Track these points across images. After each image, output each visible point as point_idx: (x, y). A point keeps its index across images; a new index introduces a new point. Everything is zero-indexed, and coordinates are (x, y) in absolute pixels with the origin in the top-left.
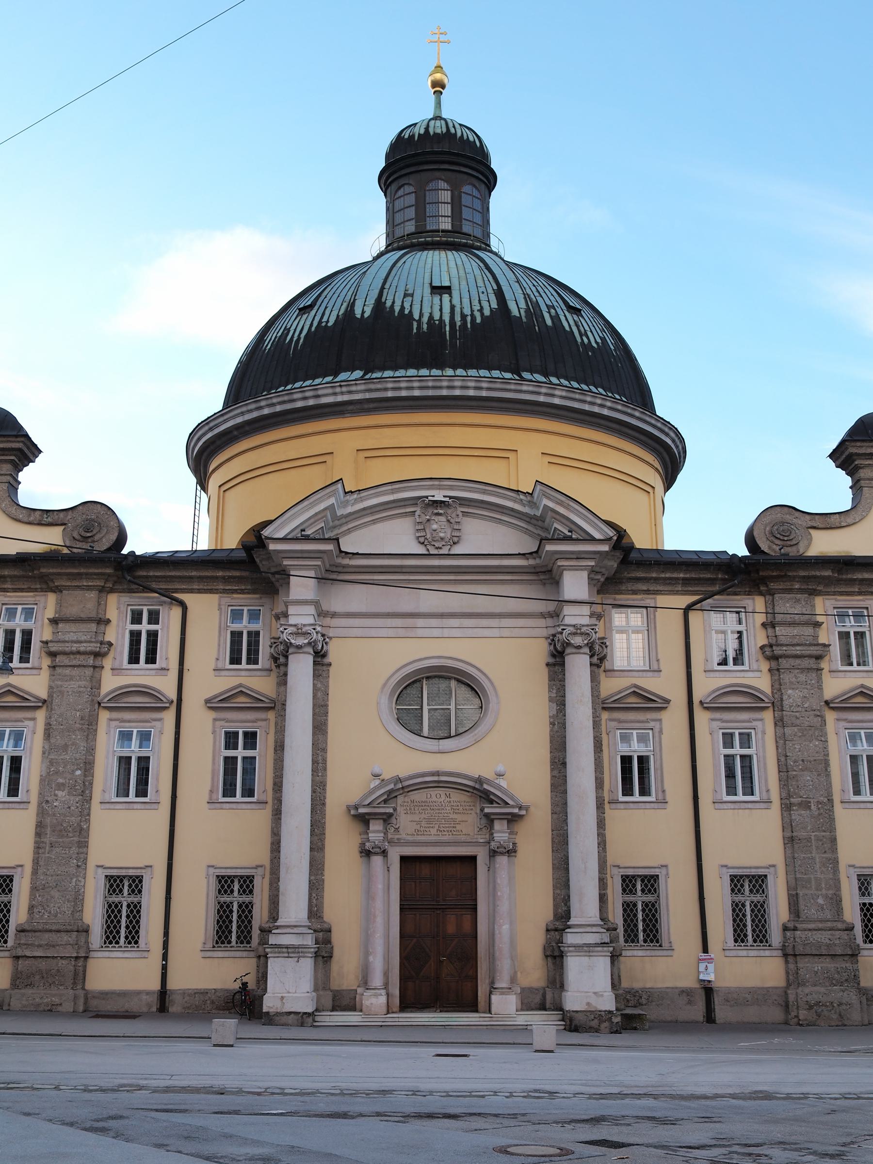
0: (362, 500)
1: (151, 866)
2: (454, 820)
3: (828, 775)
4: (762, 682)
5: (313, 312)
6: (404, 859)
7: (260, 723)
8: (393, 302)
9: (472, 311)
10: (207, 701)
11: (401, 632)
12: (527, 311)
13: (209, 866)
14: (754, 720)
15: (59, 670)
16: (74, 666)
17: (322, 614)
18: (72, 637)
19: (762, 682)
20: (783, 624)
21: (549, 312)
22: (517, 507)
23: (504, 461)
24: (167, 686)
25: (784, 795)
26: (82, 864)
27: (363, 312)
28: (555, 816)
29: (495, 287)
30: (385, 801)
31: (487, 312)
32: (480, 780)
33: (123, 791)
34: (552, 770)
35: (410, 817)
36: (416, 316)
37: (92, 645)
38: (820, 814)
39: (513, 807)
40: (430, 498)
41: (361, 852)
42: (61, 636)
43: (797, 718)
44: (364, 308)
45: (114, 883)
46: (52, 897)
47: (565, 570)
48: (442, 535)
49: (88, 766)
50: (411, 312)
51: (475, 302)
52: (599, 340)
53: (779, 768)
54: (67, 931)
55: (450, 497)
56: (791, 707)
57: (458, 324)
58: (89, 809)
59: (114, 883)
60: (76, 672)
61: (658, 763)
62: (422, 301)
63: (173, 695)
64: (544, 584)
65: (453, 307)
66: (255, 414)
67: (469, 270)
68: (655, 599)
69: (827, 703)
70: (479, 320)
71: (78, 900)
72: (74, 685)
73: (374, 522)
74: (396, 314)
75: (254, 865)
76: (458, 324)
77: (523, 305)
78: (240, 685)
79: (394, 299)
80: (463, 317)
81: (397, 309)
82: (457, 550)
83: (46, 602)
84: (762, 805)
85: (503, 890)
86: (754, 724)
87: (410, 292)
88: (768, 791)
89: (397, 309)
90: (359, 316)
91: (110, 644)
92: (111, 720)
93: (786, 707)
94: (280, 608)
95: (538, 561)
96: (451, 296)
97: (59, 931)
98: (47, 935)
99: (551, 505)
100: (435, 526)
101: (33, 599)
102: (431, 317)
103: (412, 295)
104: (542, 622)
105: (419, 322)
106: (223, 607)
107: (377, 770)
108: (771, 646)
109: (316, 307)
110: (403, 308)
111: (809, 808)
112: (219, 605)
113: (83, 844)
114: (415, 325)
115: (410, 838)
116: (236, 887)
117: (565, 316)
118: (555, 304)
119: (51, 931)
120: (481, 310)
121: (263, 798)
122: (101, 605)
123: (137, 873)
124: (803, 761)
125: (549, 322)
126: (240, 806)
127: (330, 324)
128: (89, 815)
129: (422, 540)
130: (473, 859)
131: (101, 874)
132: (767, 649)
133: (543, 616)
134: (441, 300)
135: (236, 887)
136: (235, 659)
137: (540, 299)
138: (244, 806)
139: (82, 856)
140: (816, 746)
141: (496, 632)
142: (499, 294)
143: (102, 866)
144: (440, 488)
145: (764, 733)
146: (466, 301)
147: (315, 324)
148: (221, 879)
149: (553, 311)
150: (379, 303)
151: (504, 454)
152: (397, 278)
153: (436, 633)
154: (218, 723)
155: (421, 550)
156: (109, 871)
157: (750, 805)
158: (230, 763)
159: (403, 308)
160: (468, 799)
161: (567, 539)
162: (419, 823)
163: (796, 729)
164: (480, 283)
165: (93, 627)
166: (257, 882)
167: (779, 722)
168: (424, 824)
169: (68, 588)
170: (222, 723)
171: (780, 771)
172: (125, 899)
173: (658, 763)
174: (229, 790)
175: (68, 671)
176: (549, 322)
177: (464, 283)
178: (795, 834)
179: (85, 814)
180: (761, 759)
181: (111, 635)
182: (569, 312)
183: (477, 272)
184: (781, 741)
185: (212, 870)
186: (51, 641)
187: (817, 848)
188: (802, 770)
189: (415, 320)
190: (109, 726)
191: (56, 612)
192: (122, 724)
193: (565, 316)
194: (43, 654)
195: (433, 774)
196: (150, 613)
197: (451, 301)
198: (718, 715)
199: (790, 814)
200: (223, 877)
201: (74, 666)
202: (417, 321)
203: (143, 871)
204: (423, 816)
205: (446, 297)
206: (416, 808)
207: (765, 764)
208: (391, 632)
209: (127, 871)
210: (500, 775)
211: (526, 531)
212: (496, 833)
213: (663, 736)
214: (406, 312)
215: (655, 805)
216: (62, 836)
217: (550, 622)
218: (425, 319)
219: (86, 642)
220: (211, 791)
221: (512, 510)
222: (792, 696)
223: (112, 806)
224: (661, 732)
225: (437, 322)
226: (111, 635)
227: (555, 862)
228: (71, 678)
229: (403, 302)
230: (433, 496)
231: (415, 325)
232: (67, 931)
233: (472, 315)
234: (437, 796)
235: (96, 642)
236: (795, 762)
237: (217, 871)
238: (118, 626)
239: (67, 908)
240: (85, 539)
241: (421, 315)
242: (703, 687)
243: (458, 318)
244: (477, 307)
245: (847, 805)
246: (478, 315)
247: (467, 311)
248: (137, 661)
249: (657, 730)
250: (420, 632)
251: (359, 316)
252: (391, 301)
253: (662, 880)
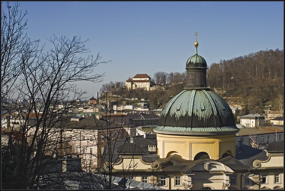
5: (180, 111)
27: (190, 115)
31: (211, 115)
36: (199, 117)
44: (190, 114)
65: (205, 114)
79: (195, 112)
81: (196, 114)
89: (196, 114)
102: (202, 116)
109: (180, 110)
110: (197, 114)
120: (210, 115)
127: (184, 116)
142: (212, 109)
147: (181, 115)
159: (197, 114)
164: (209, 108)
196: (164, 177)
214: (197, 115)
218: (201, 117)
243: (206, 117)
246: (209, 115)
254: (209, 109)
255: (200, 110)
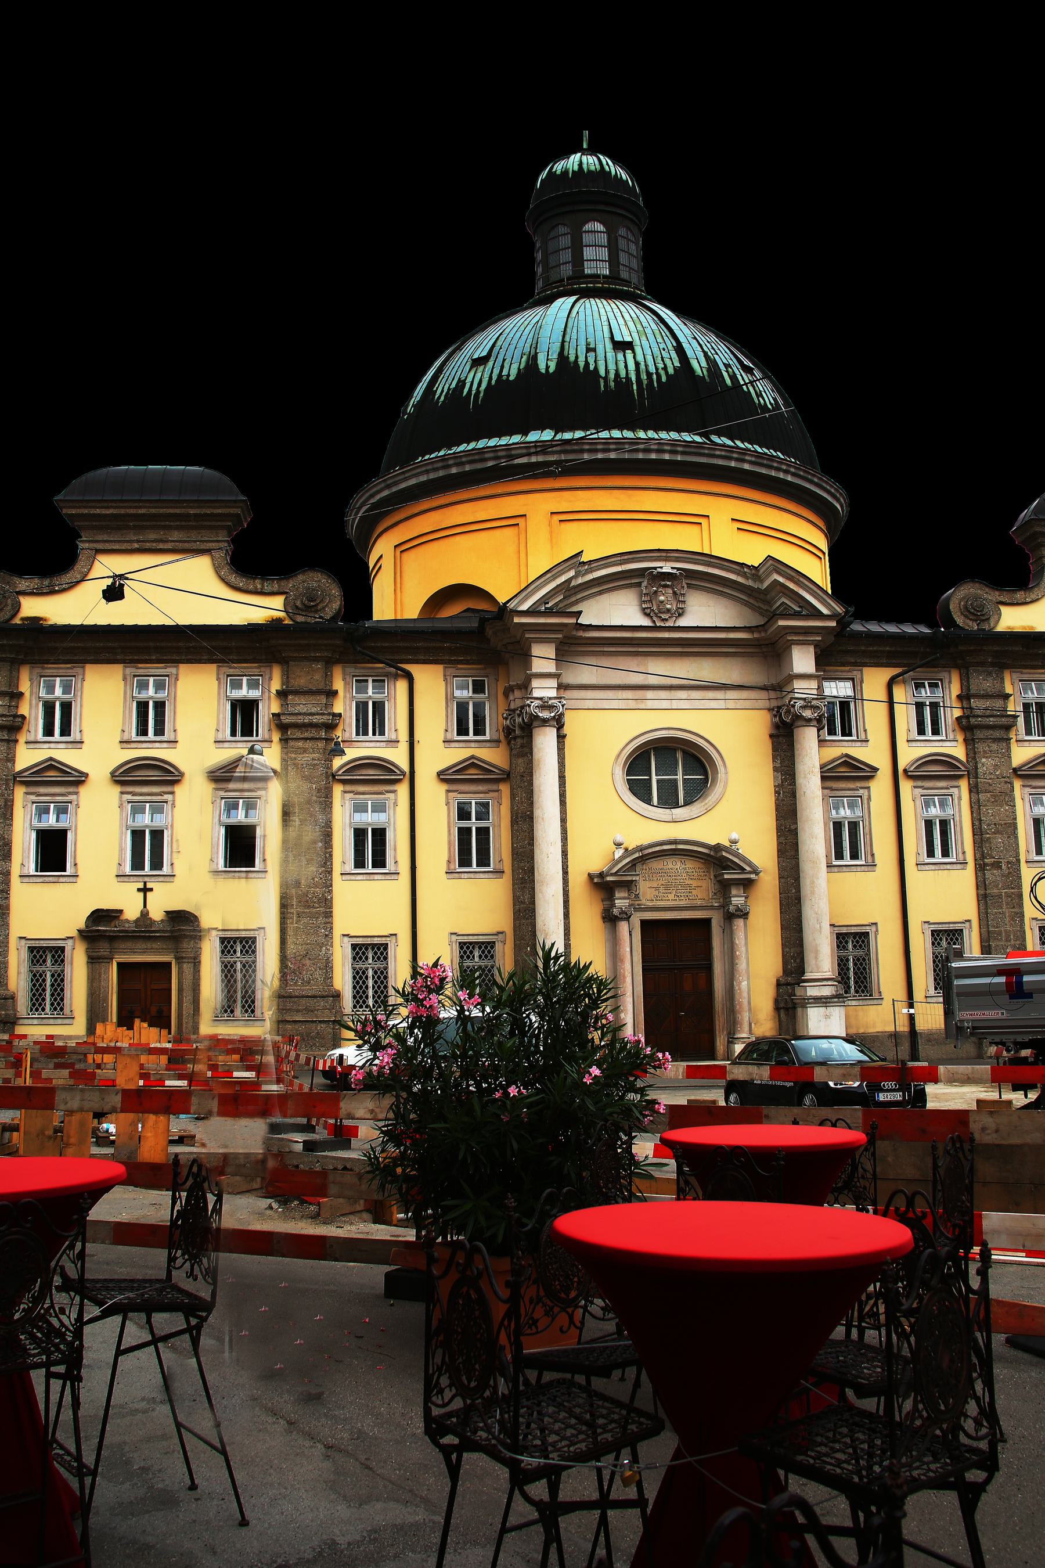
0: (592, 571)
1: (396, 935)
2: (690, 886)
3: (1016, 838)
4: (958, 751)
5: (490, 364)
6: (644, 923)
7: (491, 794)
8: (577, 357)
9: (657, 369)
10: (439, 774)
11: (632, 704)
12: (709, 370)
13: (451, 934)
14: (951, 787)
15: (291, 743)
16: (306, 739)
17: (561, 687)
18: (302, 709)
19: (958, 751)
20: (977, 696)
21: (727, 371)
22: (740, 579)
23: (696, 528)
24: (399, 756)
25: (978, 856)
26: (329, 936)
27: (547, 367)
28: (782, 880)
29: (675, 345)
30: (628, 870)
31: (671, 371)
32: (718, 848)
33: (360, 863)
34: (778, 837)
35: (648, 884)
36: (602, 373)
37: (325, 717)
38: (1009, 873)
39: (750, 873)
40: (659, 570)
41: (604, 918)
42: (291, 709)
43: (990, 785)
44: (547, 362)
45: (359, 950)
46: (303, 965)
47: (794, 644)
48: (668, 606)
49: (327, 836)
50: (596, 368)
51: (659, 360)
52: (772, 402)
53: (973, 831)
54: (323, 997)
55: (678, 569)
56: (984, 774)
57: (645, 382)
58: (331, 880)
59: (359, 950)
60: (308, 744)
61: (867, 828)
62: (605, 357)
63: (405, 766)
64: (765, 657)
65: (637, 364)
66: (441, 473)
67: (645, 324)
68: (861, 671)
69: (1015, 770)
70: (664, 379)
71: (327, 967)
72: (307, 758)
73: (601, 593)
74: (582, 370)
75: (494, 931)
76: (645, 382)
77: (704, 364)
78: (473, 757)
79: (577, 353)
80: (649, 375)
81: (582, 364)
82: (683, 622)
83: (271, 674)
84: (959, 866)
85: (741, 951)
86: (952, 790)
87: (592, 346)
88: (964, 853)
89: (582, 364)
90: (543, 371)
91: (340, 715)
92: (345, 792)
93: (980, 775)
94: (516, 679)
95: (763, 634)
96: (634, 352)
97: (314, 997)
98: (303, 1001)
99: (781, 580)
100: (662, 598)
101: (258, 670)
102: (617, 374)
103: (594, 350)
104: (763, 694)
105: (606, 379)
106: (448, 678)
107: (619, 839)
108: (968, 717)
109: (492, 359)
110: (587, 364)
111: (1001, 867)
112: (445, 676)
113: (329, 914)
114: (602, 384)
115: (650, 904)
116: (477, 954)
117: (741, 375)
118: (731, 362)
119: (307, 997)
120: (665, 368)
121: (499, 867)
122: (328, 677)
123: (383, 941)
124: (995, 824)
125: (728, 381)
126: (477, 876)
127: (512, 378)
128: (331, 886)
129: (648, 611)
130: (707, 922)
131: (347, 943)
132: (964, 721)
133: (764, 688)
134: (625, 356)
135: (477, 954)
136: (462, 730)
137: (716, 356)
138: (482, 875)
139: (328, 926)
140: (1006, 810)
141: (721, 704)
142: (680, 349)
143: (347, 935)
144: (667, 559)
145: (960, 798)
146: (649, 358)
148: (462, 945)
149: (730, 369)
150: (562, 357)
151: (697, 519)
152: (575, 331)
153: (665, 704)
154: (450, 794)
155: (646, 622)
156: (355, 939)
157: (948, 867)
158: (464, 834)
159: (587, 364)
160: (701, 866)
161: (796, 615)
162: (657, 889)
163: (989, 795)
164: (660, 340)
165: (323, 699)
166: (498, 947)
167: (974, 789)
168: (662, 890)
169: (295, 659)
170: (455, 794)
171: (974, 835)
172: (370, 965)
173: (867, 828)
174: (465, 861)
175: (300, 744)
176: (728, 381)
177: (644, 338)
178: (988, 892)
179: (329, 886)
180: (958, 823)
181: (338, 707)
182: (744, 371)
183: (654, 326)
184: (976, 807)
185: (454, 937)
186: (283, 714)
187: (1007, 904)
188: (994, 833)
189: (601, 377)
190: (343, 798)
191: (283, 684)
192: (357, 796)
193: (741, 375)
194: (273, 727)
195: (670, 842)
197: (634, 357)
198: (919, 783)
199: (984, 874)
200: (465, 943)
201: (306, 739)
202: (603, 378)
203: (388, 939)
204: (661, 882)
205: (629, 354)
206: (654, 875)
207: (961, 828)
208: (622, 704)
209: (372, 939)
210: (734, 842)
211: (746, 604)
212: (734, 897)
213: (871, 803)
214: (592, 368)
215: (866, 868)
216: (309, 907)
217: (773, 694)
218: (612, 376)
219: (318, 714)
220: (449, 862)
221: (735, 582)
222: (986, 764)
223: (353, 877)
224: (869, 798)
225: (624, 380)
226: (338, 707)
227: (784, 923)
228: (305, 751)
229: (586, 357)
230: (661, 568)
231: (602, 384)
232: (323, 997)
233: (657, 374)
234: (674, 865)
235: (329, 714)
236: (989, 825)
237: (459, 937)
238: (345, 697)
239: (318, 975)
240: (307, 609)
241: (607, 371)
242: (908, 755)
243: (644, 376)
244: (661, 366)
245: (1031, 865)
246: (662, 373)
247: (652, 369)
248: (366, 733)
249: (865, 798)
250: (650, 704)
251: (543, 371)
252: (574, 356)
253: (872, 937)
254: (662, 346)
255: (604, 347)
